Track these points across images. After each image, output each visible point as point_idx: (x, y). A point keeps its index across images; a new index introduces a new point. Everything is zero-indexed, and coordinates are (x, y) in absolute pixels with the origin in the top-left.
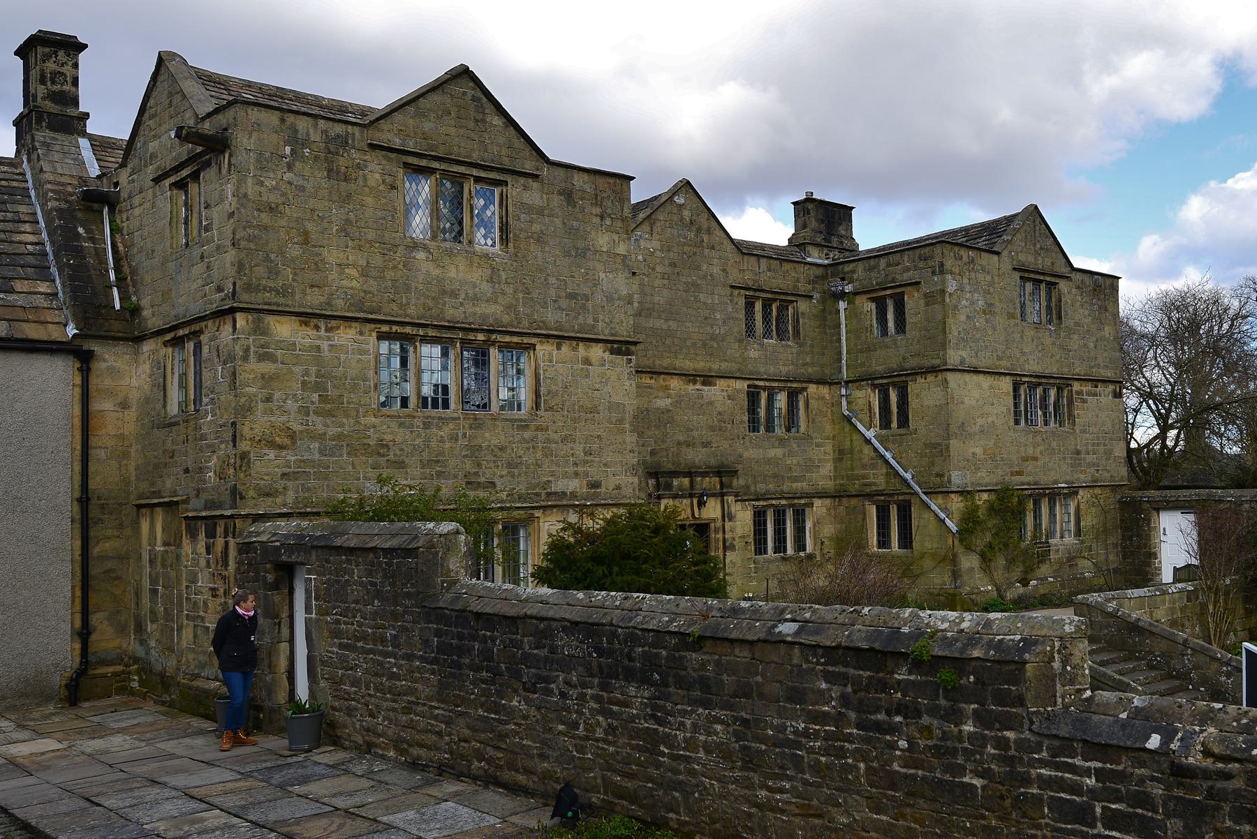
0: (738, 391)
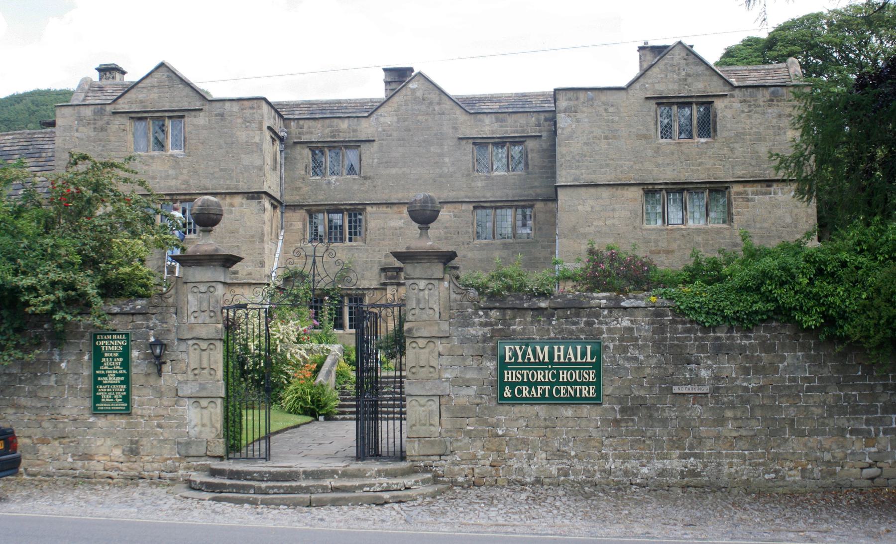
0: (464, 211)
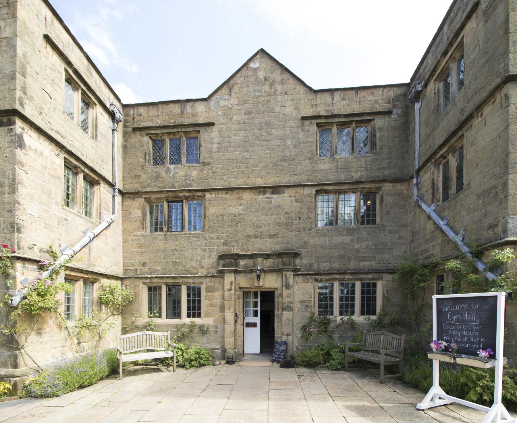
0: (306, 196)
